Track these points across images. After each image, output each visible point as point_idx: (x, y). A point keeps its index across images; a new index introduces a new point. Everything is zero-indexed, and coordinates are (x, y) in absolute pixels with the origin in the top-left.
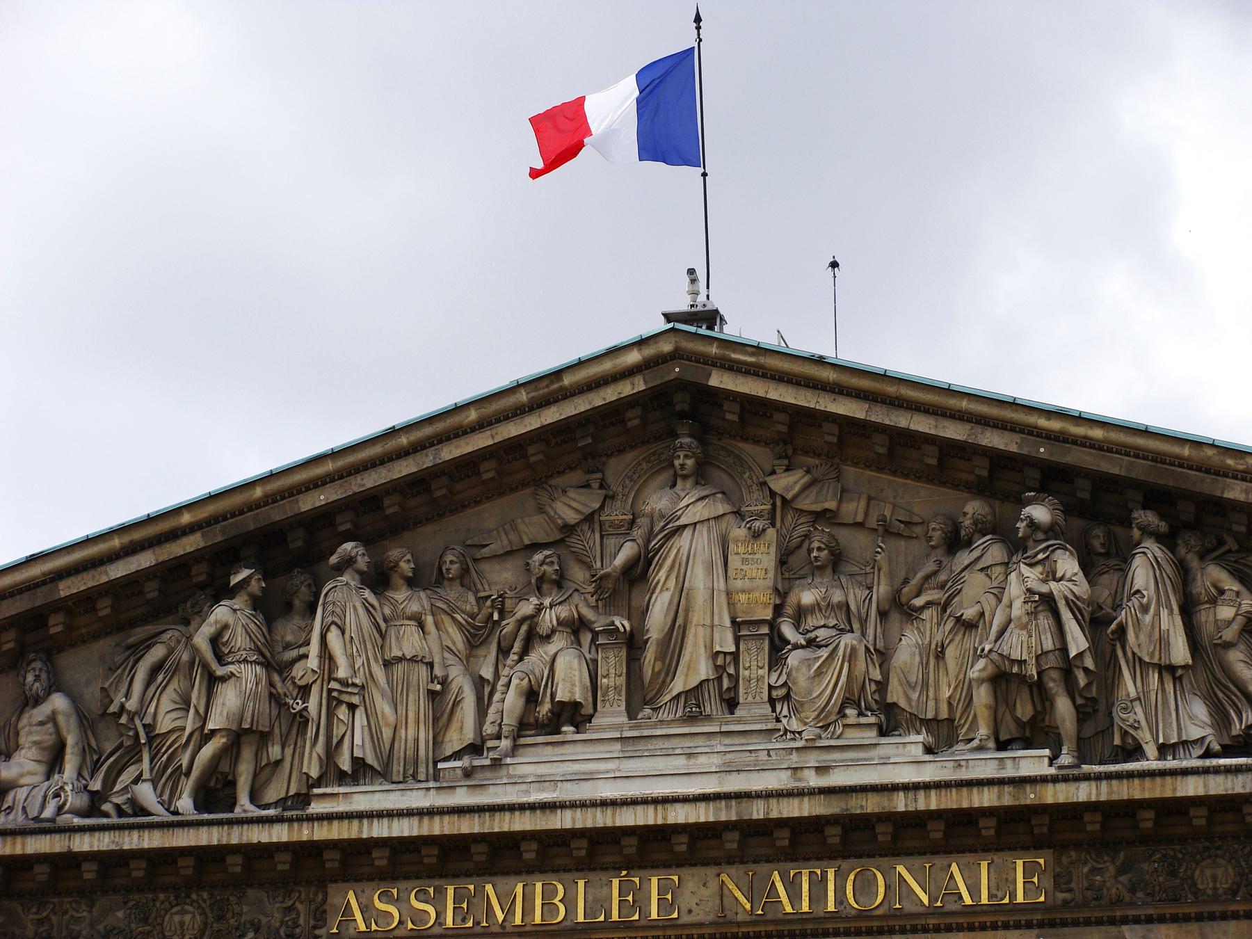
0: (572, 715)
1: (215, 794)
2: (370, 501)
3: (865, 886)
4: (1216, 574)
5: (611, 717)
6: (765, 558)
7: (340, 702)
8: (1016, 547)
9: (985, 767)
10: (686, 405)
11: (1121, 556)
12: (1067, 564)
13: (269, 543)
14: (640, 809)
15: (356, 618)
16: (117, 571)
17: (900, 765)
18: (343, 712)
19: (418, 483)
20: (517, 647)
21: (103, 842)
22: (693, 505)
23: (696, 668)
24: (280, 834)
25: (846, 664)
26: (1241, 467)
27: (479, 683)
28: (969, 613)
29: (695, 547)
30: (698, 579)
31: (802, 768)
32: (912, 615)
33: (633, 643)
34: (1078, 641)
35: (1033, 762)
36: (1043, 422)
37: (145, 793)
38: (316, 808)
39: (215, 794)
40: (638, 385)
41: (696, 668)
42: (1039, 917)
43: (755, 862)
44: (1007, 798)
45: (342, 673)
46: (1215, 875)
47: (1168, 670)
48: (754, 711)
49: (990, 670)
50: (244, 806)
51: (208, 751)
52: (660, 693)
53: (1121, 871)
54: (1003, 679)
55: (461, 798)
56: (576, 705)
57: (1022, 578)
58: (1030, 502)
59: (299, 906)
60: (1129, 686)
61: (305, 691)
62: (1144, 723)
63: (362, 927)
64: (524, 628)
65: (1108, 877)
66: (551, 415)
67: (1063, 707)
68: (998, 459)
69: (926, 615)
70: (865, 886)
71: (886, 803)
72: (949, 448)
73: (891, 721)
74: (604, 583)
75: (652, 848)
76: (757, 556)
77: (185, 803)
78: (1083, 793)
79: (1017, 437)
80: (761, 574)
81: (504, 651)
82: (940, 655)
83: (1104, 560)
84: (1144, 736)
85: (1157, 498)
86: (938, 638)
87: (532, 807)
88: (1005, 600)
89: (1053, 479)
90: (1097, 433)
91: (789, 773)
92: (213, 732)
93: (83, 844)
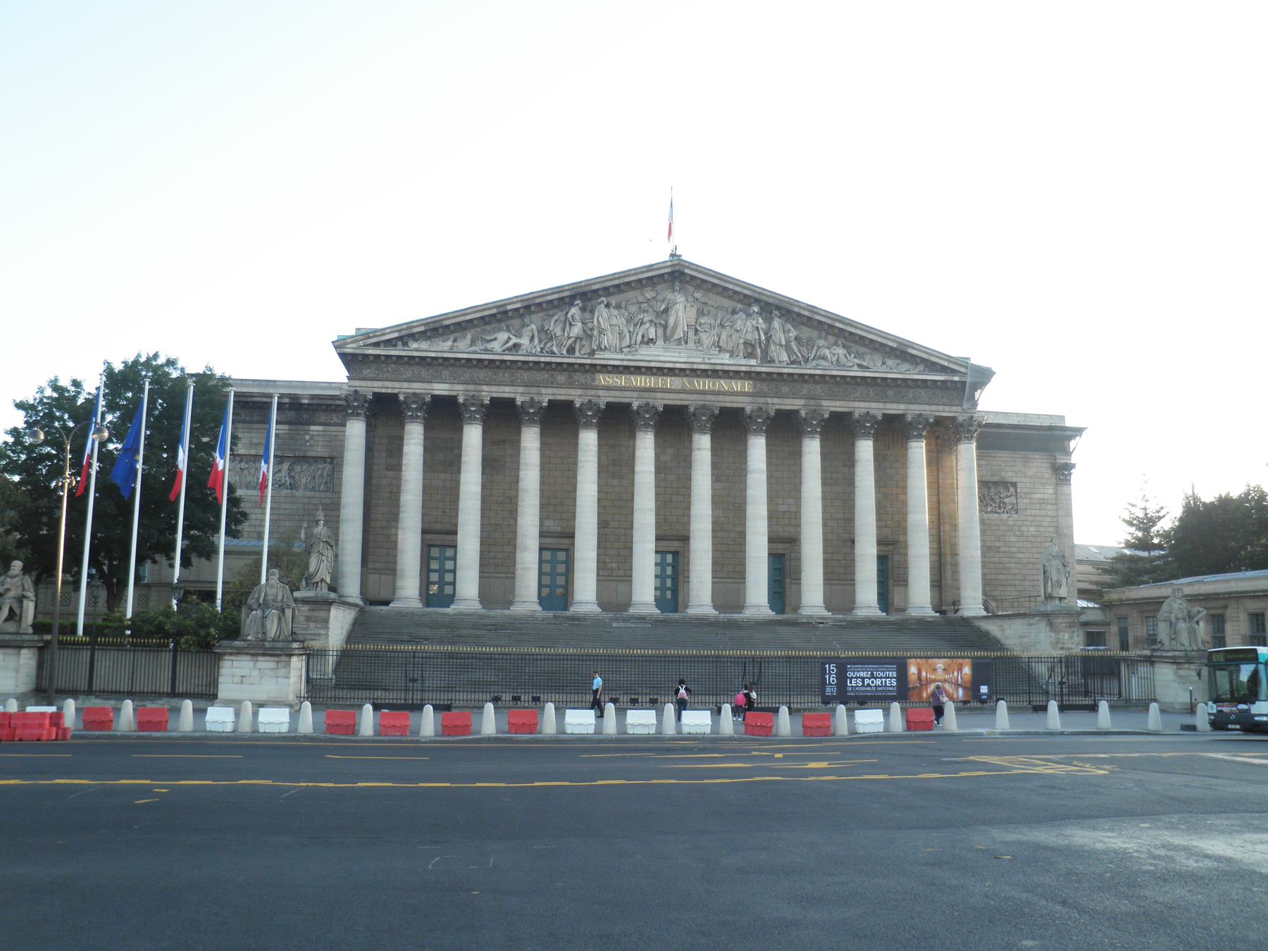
0: (651, 341)
1: (571, 350)
2: (606, 289)
3: (714, 384)
4: (789, 326)
5: (660, 342)
6: (694, 311)
8: (749, 315)
9: (743, 362)
10: (677, 275)
11: (772, 319)
12: (761, 321)
13: (585, 296)
15: (605, 315)
16: (549, 298)
17: (724, 360)
19: (618, 286)
21: (548, 359)
22: (680, 298)
24: (589, 361)
29: (680, 307)
30: (681, 314)
32: (722, 326)
33: (665, 327)
34: (763, 338)
35: (753, 362)
37: (555, 349)
39: (571, 350)
40: (669, 270)
44: (748, 369)
46: (785, 389)
48: (691, 345)
50: (577, 354)
51: (570, 341)
54: (745, 343)
55: (629, 357)
60: (772, 347)
61: (592, 329)
65: (764, 387)
66: (650, 274)
68: (746, 296)
70: (714, 384)
72: (735, 292)
73: (721, 350)
75: (671, 372)
77: (564, 352)
78: (764, 369)
81: (635, 325)
85: (778, 308)
89: (757, 301)
93: (543, 359)
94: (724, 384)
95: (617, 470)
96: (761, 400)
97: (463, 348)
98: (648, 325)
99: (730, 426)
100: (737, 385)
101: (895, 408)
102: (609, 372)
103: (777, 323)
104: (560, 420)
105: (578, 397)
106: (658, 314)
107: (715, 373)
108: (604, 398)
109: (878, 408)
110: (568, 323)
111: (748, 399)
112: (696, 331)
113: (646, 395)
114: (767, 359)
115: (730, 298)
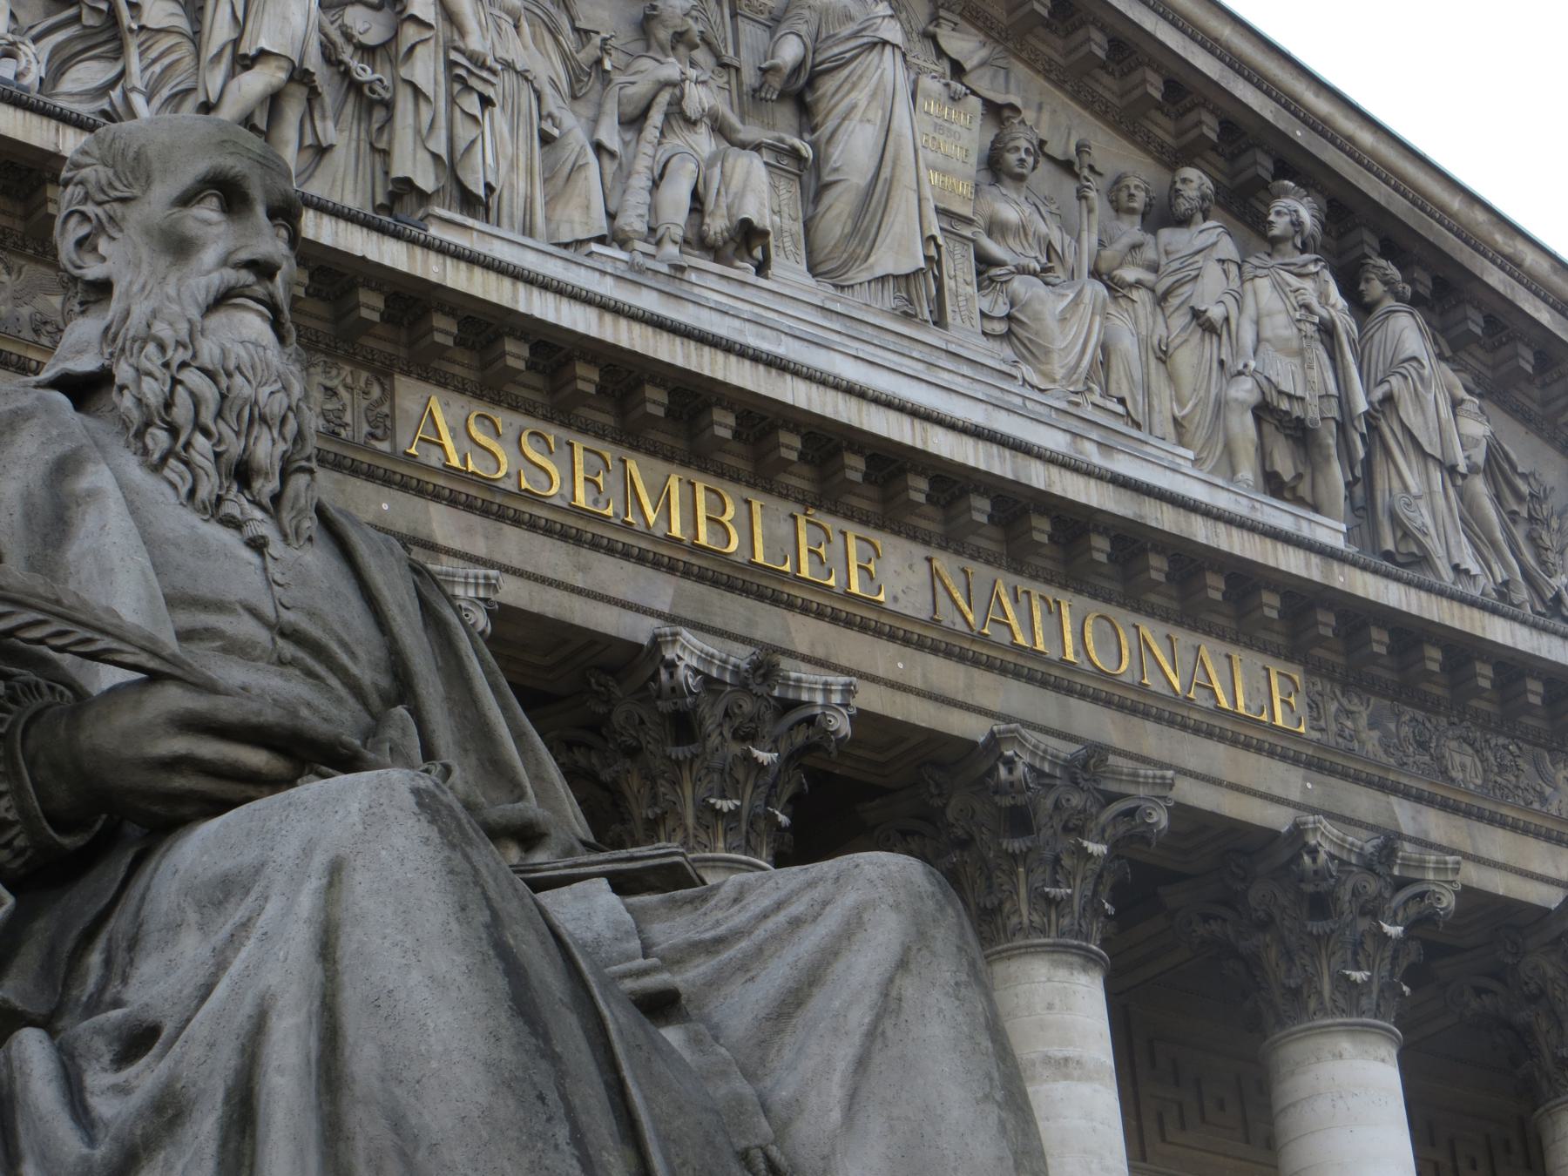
5: (789, 269)
7: (468, 88)
14: (893, 416)
18: (472, 104)
20: (656, 117)
23: (898, 250)
24: (392, 254)
25: (1098, 319)
26: (1508, 250)
27: (599, 148)
28: (1215, 313)
31: (1082, 437)
36: (1309, 97)
38: (435, 231)
41: (898, 250)
42: (1310, 752)
43: (973, 558)
45: (475, 42)
46: (1464, 765)
47: (1452, 470)
49: (1253, 398)
52: (845, 266)
53: (1372, 725)
54: (1263, 411)
55: (648, 301)
56: (748, 239)
57: (1278, 286)
58: (1285, 193)
59: (342, 391)
62: (1432, 531)
63: (455, 462)
64: (664, 97)
65: (1366, 728)
67: (1337, 474)
69: (1135, 295)
71: (1184, 525)
74: (770, 77)
76: (954, 127)
78: (1393, 595)
79: (1272, 105)
80: (959, 153)
82: (1164, 356)
84: (1435, 546)
86: (1161, 330)
87: (756, 357)
88: (1250, 310)
90: (1366, 138)
91: (1068, 437)
92: (263, 54)
96: (1363, 803)
98: (704, 142)
102: (491, 389)
103: (1407, 333)
106: (754, 100)
111: (1292, 782)
112: (984, 262)
113: (733, 610)
115: (1127, 121)
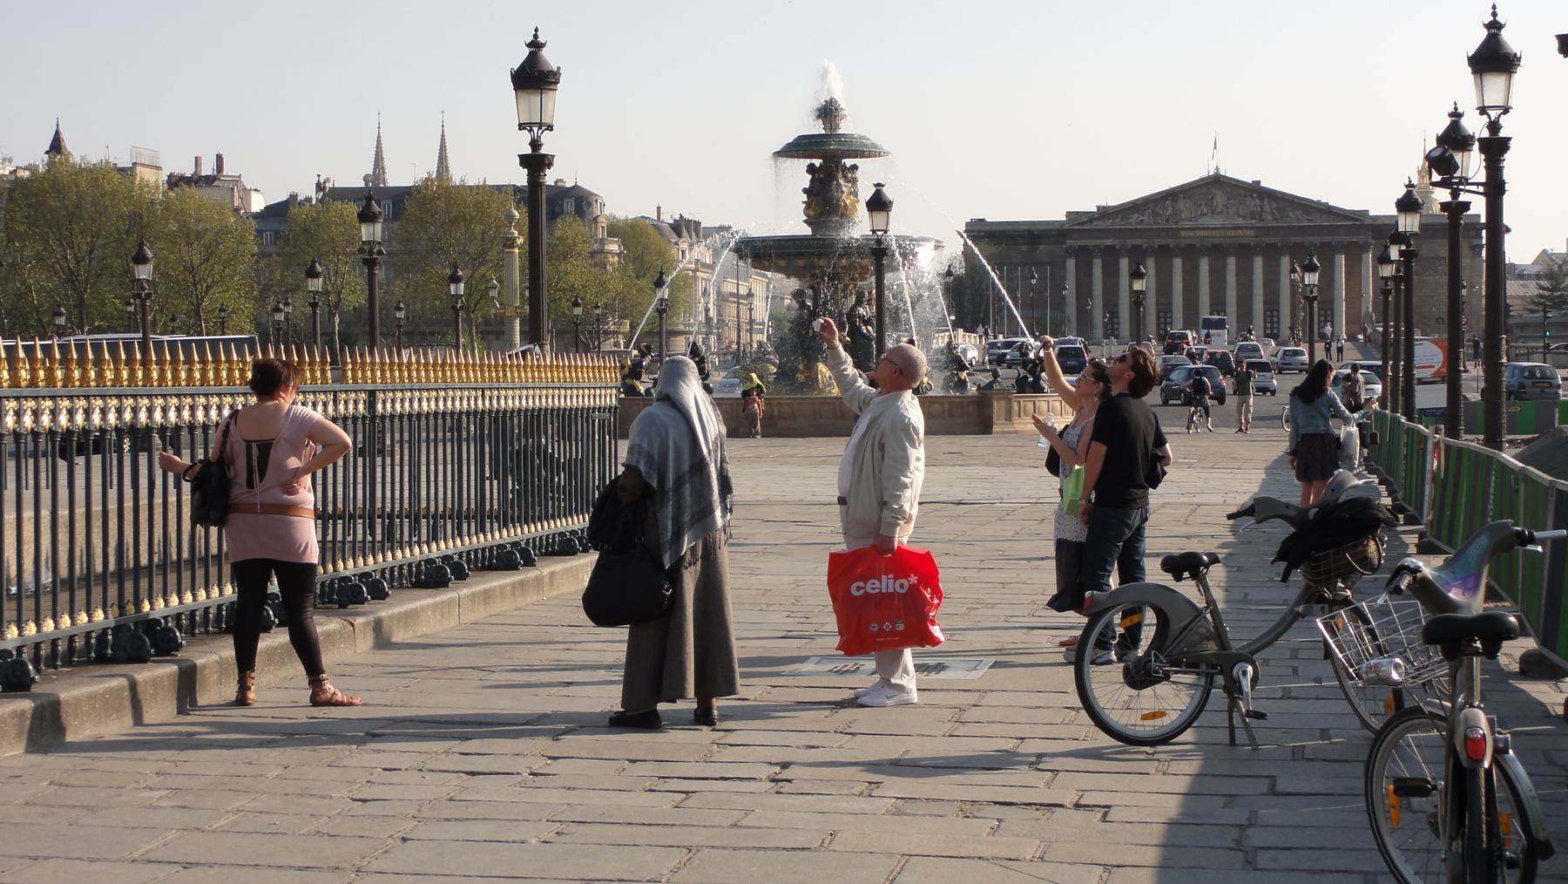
13: (1173, 195)
17: (1240, 222)
22: (1219, 193)
83: (1261, 199)
94: (1241, 233)
95: (1191, 275)
97: (1117, 224)
99: (1244, 252)
100: (1247, 233)
101: (1327, 239)
104: (1164, 254)
105: (1171, 242)
107: (1236, 228)
108: (1185, 242)
109: (1317, 239)
110: (1165, 209)
114: (1261, 220)
